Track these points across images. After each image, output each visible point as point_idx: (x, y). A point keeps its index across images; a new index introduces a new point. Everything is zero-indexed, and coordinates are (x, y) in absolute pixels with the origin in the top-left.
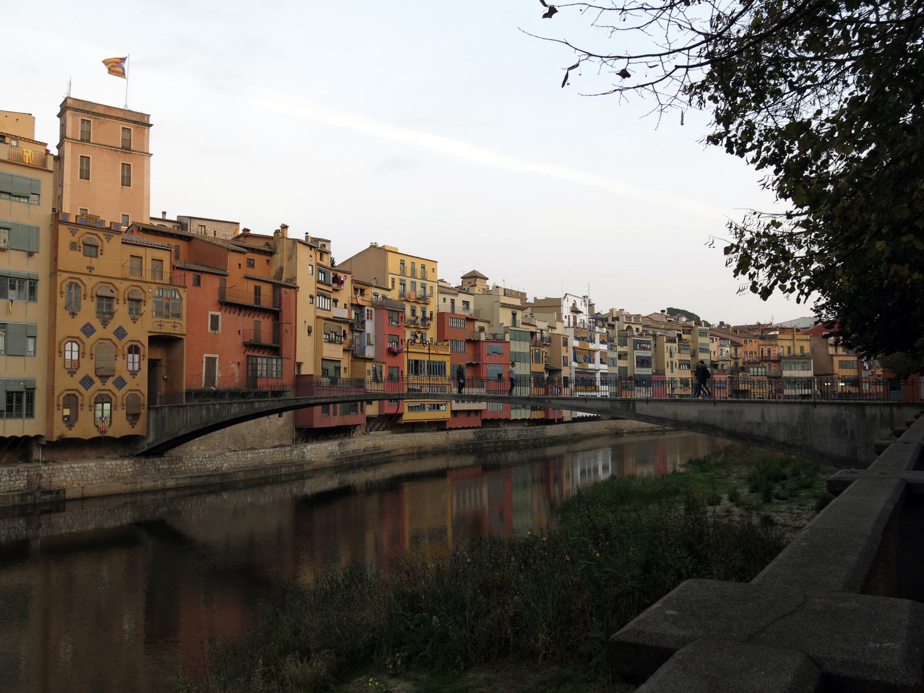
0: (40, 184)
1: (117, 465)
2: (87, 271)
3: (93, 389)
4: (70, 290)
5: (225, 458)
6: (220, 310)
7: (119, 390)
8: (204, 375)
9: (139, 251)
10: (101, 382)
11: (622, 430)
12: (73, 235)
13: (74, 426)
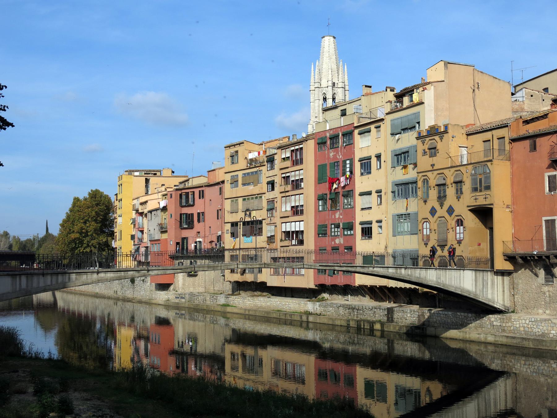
0: (419, 114)
2: (431, 168)
4: (424, 185)
5: (552, 325)
8: (544, 238)
12: (423, 145)
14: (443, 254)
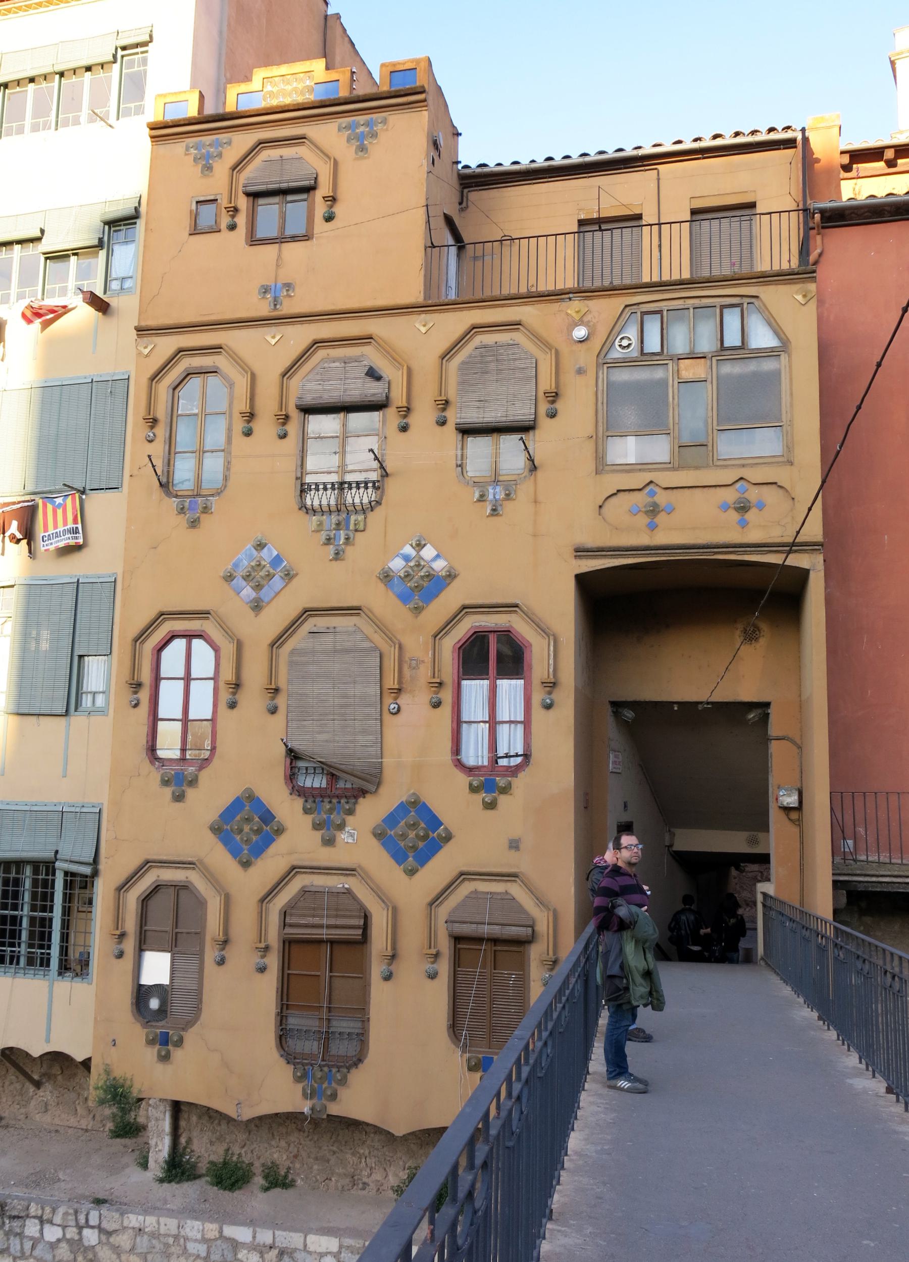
2: (263, 309)
7: (411, 872)
10: (317, 826)
13: (180, 1043)
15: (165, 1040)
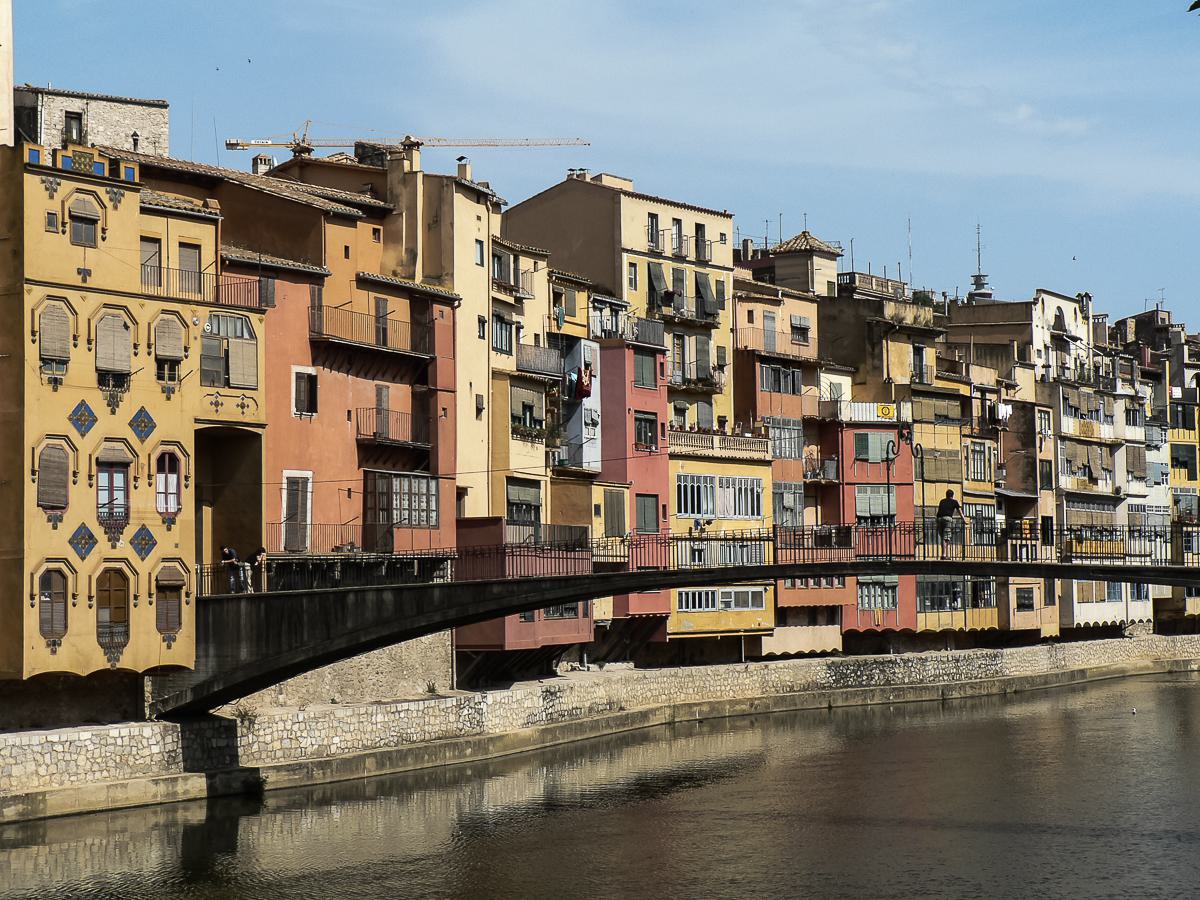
1: (132, 737)
2: (77, 280)
3: (94, 556)
6: (314, 363)
9: (156, 226)
11: (1187, 662)
12: (51, 197)
13: (60, 645)
14: (115, 554)
15: (54, 644)
